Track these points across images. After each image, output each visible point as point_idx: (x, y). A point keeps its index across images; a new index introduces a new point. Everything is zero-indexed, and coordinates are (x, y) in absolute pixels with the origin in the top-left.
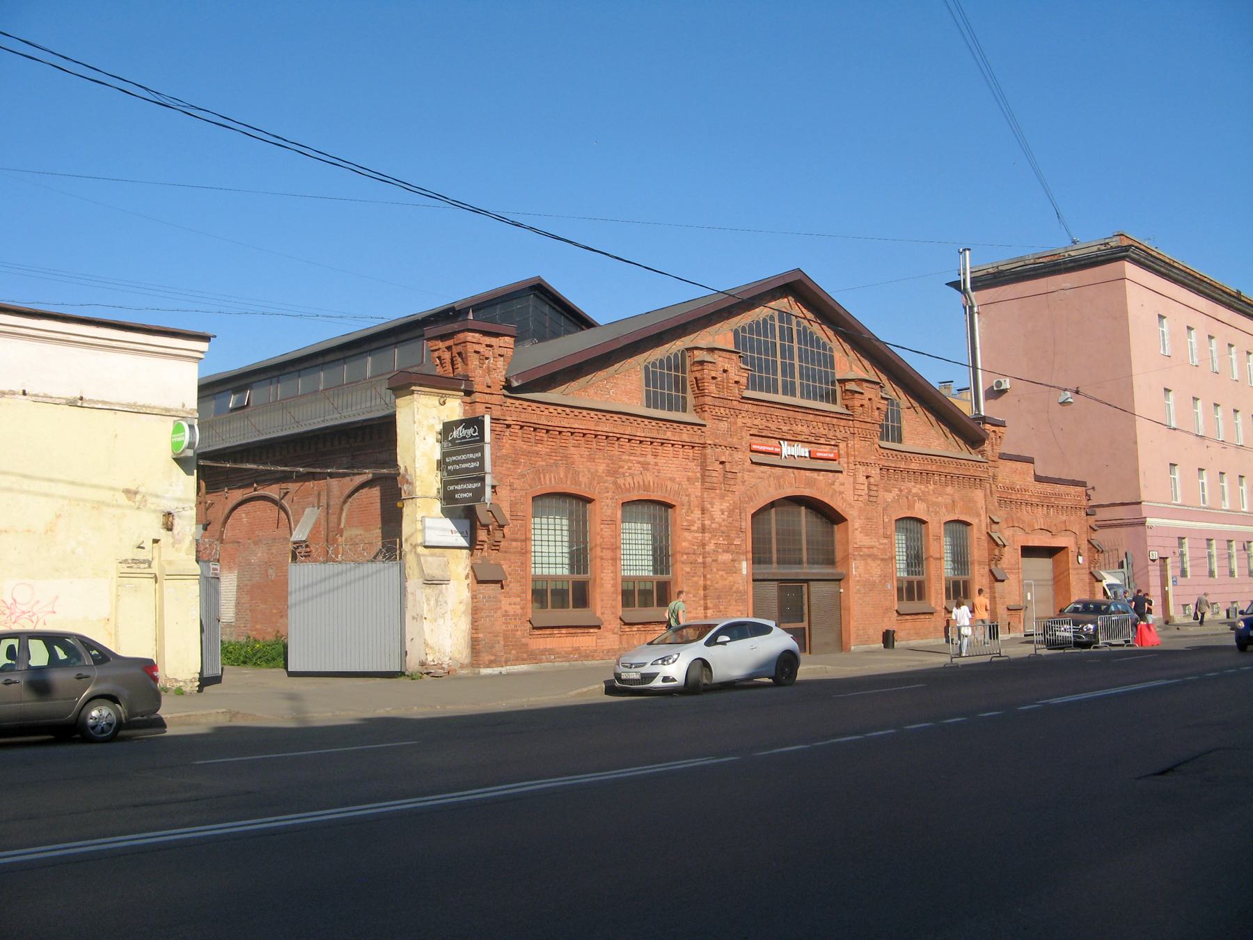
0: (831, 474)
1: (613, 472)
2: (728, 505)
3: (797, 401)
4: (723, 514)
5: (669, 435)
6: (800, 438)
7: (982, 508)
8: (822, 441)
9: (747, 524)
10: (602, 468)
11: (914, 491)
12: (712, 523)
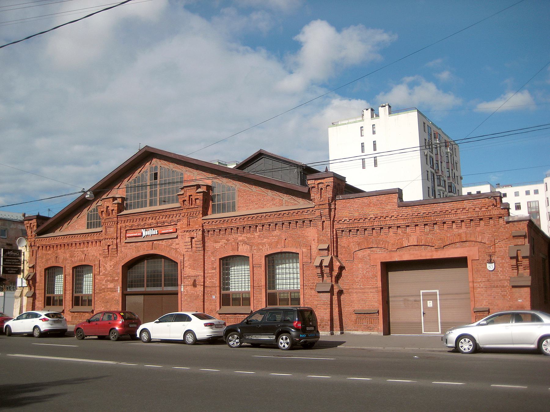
0: (170, 240)
1: (71, 256)
2: (114, 263)
3: (158, 207)
4: (111, 267)
5: (89, 238)
6: (152, 226)
7: (314, 240)
8: (166, 224)
9: (120, 270)
10: (68, 255)
11: (240, 238)
12: (106, 271)
